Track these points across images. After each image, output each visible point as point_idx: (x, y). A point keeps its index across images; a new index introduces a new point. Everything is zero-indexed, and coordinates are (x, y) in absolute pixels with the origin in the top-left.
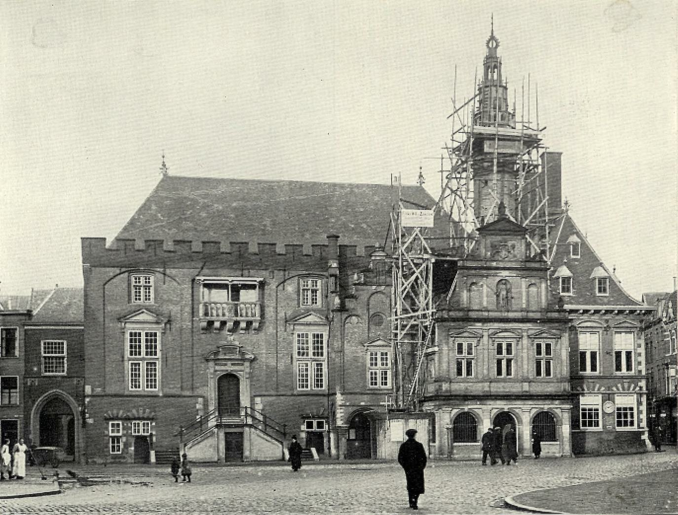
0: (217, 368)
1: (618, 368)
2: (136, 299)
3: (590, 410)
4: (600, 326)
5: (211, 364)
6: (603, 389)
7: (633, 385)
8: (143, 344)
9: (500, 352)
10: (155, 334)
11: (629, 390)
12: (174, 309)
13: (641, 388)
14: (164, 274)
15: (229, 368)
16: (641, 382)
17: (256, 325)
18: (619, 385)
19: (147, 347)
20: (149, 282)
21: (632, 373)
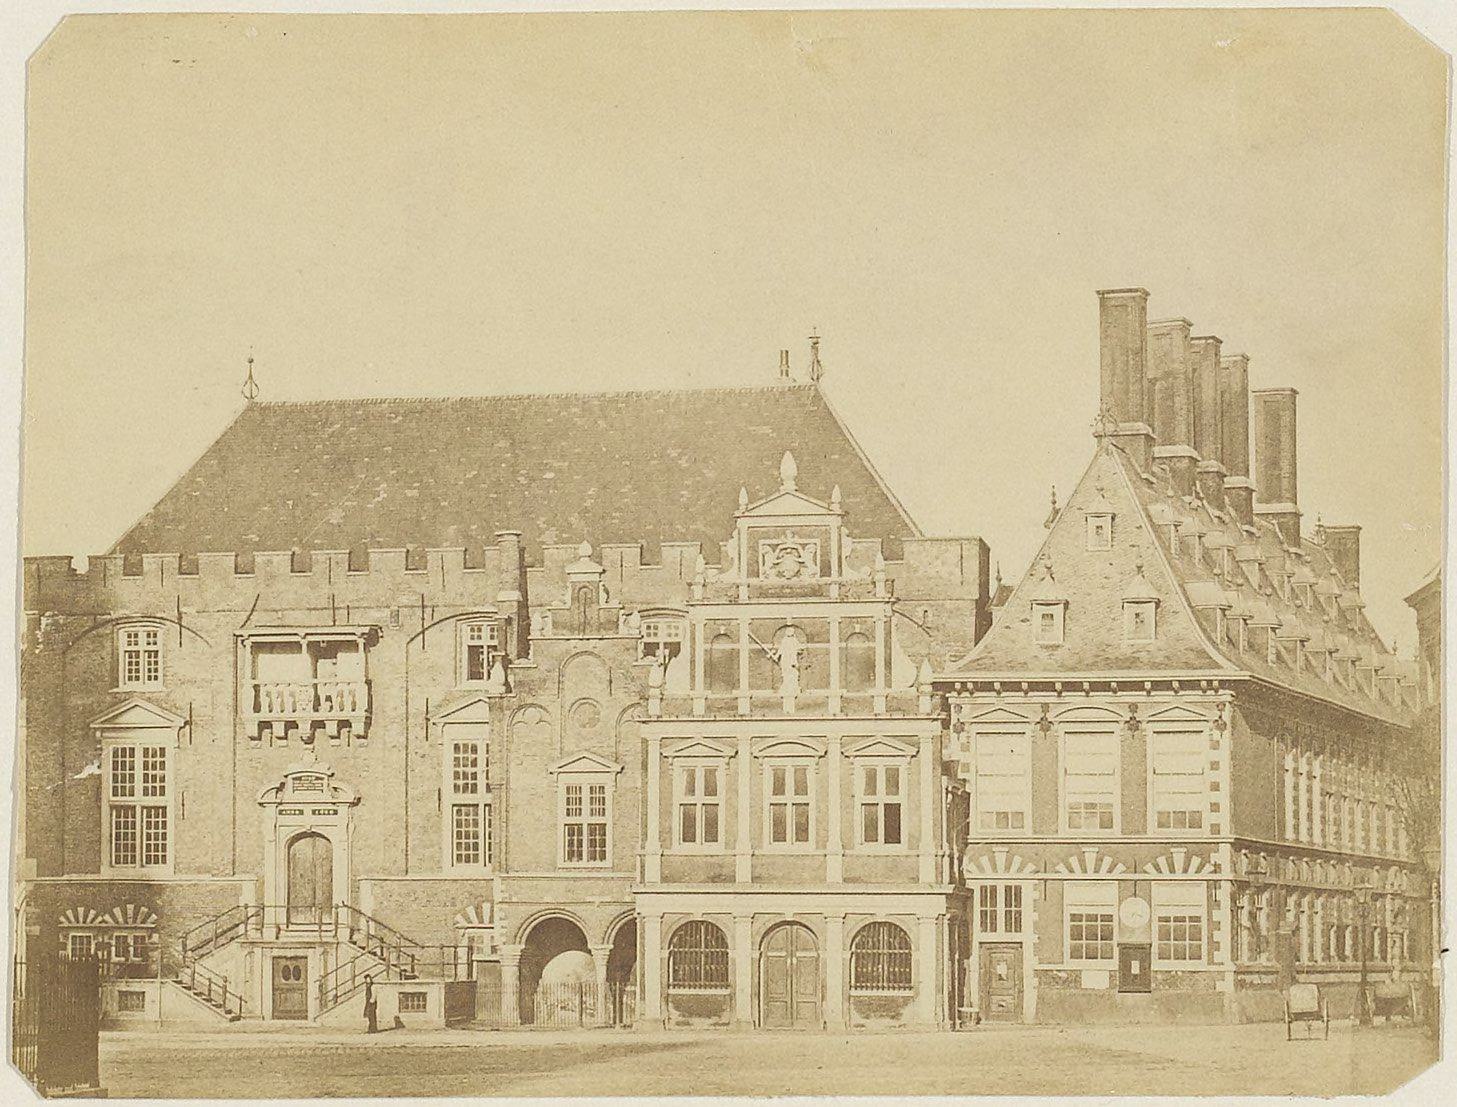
0: (282, 819)
2: (150, 678)
3: (1092, 918)
4: (1115, 717)
5: (271, 810)
6: (1121, 867)
7: (1196, 861)
8: (139, 773)
9: (779, 789)
10: (162, 750)
11: (1185, 871)
12: (199, 698)
14: (181, 626)
15: (308, 822)
17: (358, 728)
18: (1162, 861)
19: (146, 781)
20: (155, 643)
21: (1204, 834)
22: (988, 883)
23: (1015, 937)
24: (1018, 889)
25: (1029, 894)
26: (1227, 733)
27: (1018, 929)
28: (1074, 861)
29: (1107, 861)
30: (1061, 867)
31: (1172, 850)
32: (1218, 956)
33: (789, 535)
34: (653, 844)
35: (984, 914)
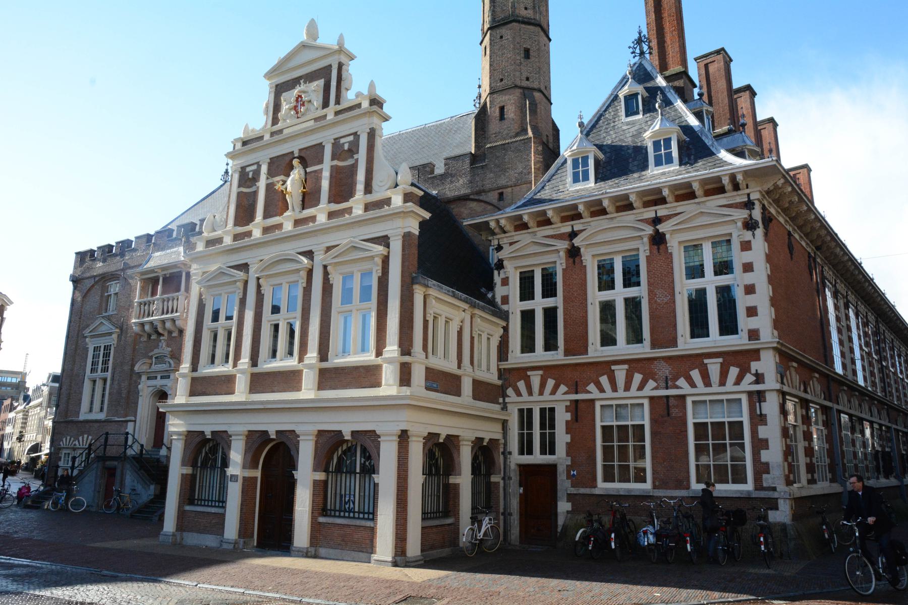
1: (699, 327)
5: (144, 378)
6: (651, 384)
7: (734, 372)
13: (759, 378)
16: (758, 359)
22: (525, 407)
23: (548, 459)
24: (552, 410)
25: (562, 417)
26: (759, 232)
27: (552, 452)
28: (604, 380)
29: (638, 378)
30: (592, 387)
31: (706, 361)
32: (767, 480)
33: (302, 83)
34: (185, 366)
35: (543, 436)
